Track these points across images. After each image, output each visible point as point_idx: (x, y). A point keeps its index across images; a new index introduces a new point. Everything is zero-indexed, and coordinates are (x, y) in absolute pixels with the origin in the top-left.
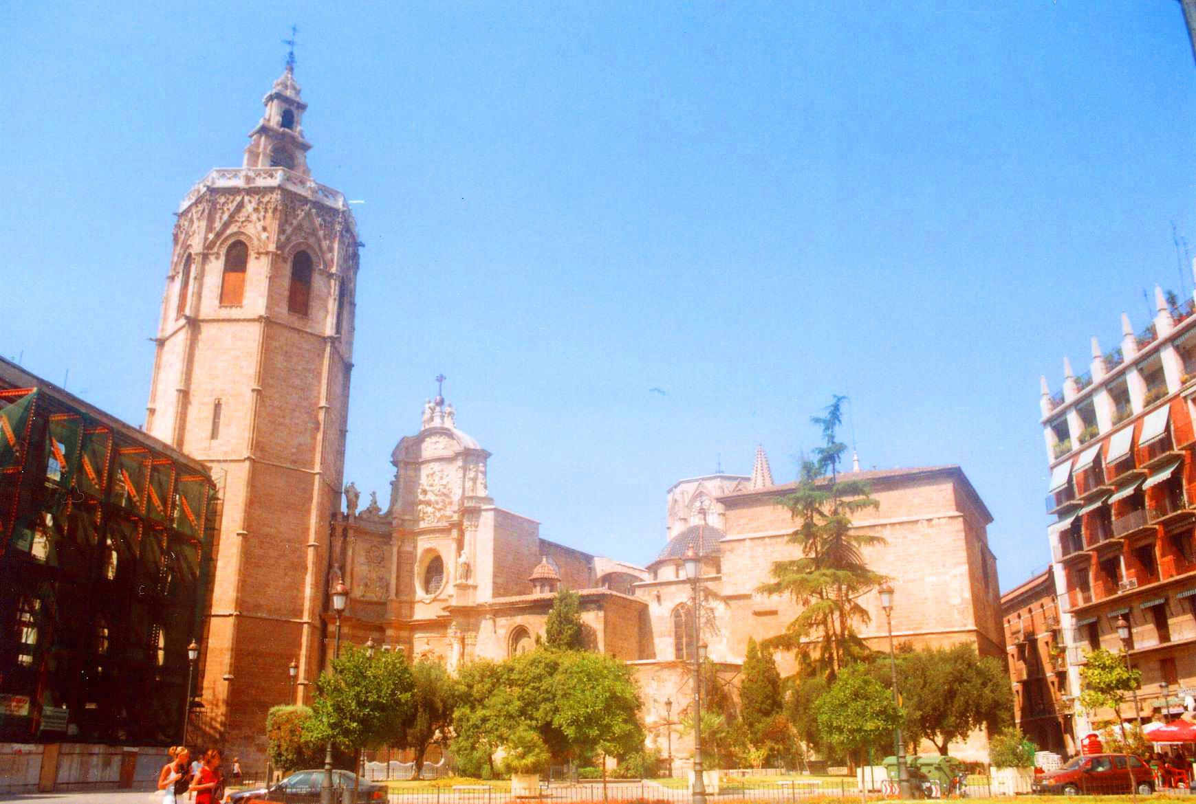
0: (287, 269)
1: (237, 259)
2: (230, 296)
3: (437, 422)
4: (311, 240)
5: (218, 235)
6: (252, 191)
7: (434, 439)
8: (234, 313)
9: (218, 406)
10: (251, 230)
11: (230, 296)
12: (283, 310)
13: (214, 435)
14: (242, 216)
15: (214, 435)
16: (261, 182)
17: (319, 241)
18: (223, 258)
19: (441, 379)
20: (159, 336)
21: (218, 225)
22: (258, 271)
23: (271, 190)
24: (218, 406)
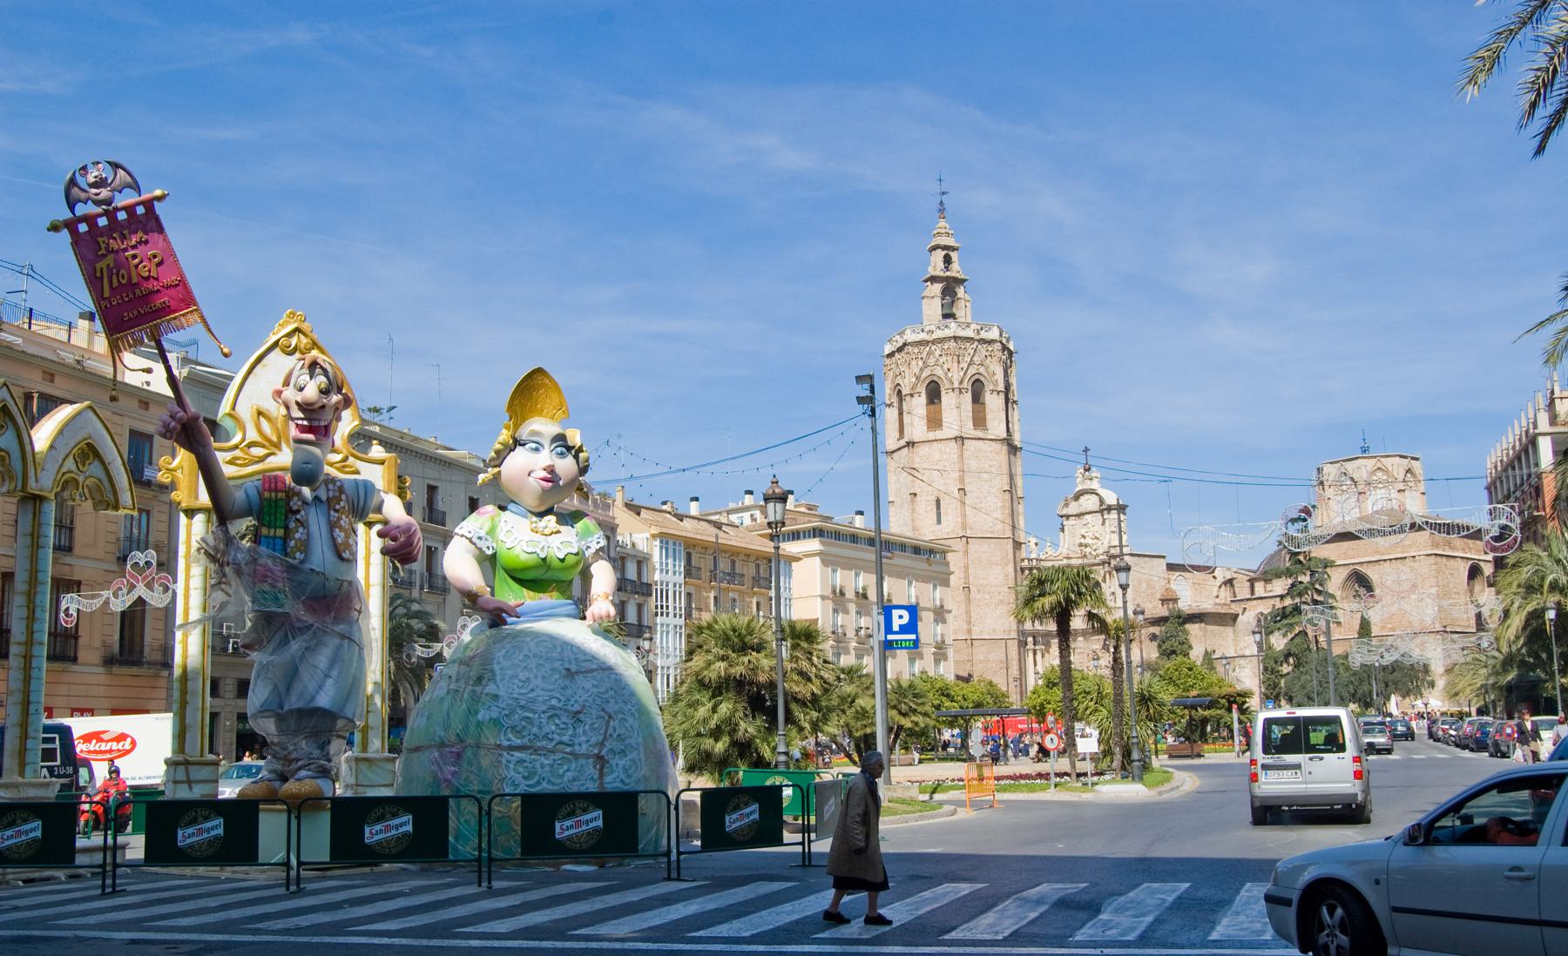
0: (968, 397)
1: (934, 393)
2: (935, 422)
3: (1088, 485)
4: (982, 370)
5: (918, 378)
6: (933, 342)
7: (1086, 497)
8: (939, 434)
9: (938, 501)
10: (939, 372)
11: (935, 422)
12: (969, 429)
13: (939, 522)
14: (932, 361)
15: (939, 522)
16: (939, 334)
17: (987, 368)
18: (924, 395)
19: (1086, 450)
20: (890, 448)
21: (917, 371)
22: (947, 399)
23: (950, 338)
24: (938, 501)
